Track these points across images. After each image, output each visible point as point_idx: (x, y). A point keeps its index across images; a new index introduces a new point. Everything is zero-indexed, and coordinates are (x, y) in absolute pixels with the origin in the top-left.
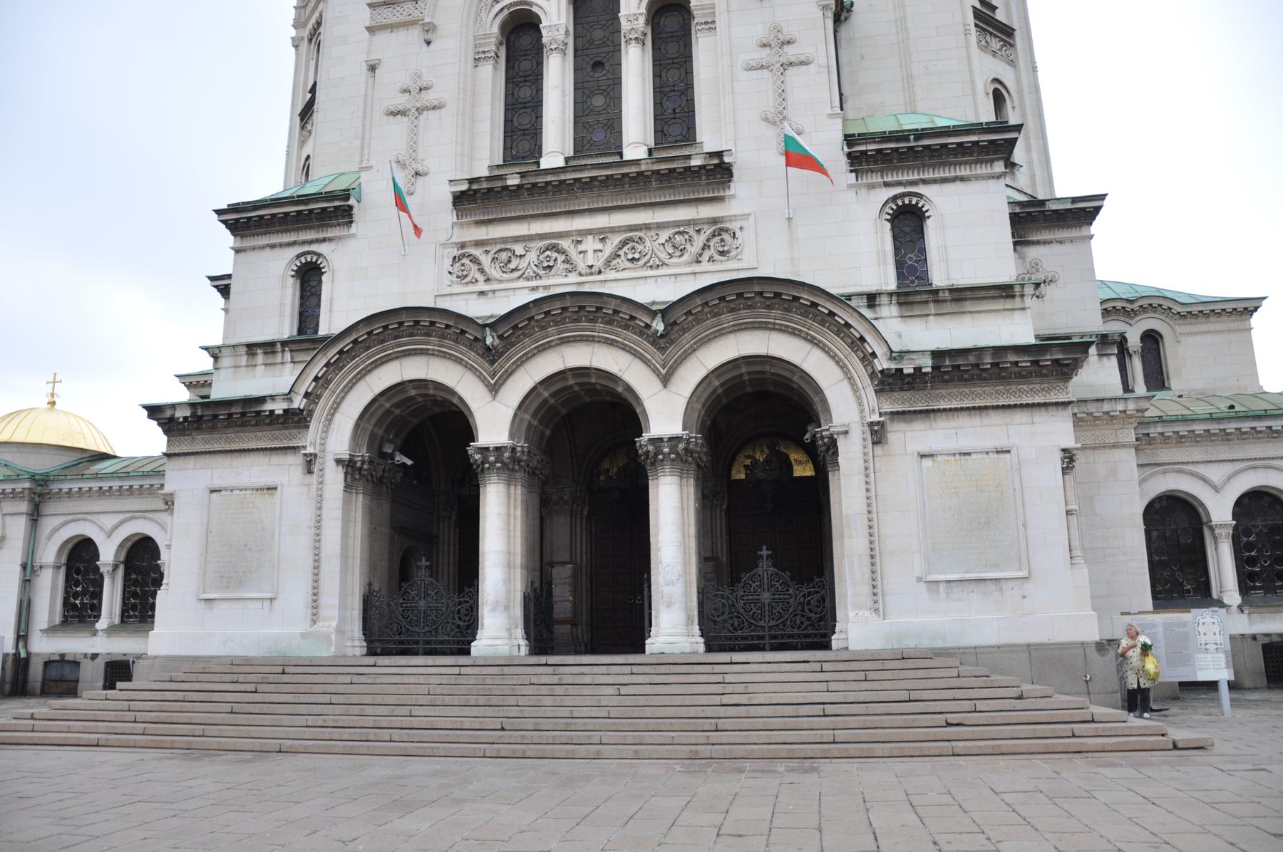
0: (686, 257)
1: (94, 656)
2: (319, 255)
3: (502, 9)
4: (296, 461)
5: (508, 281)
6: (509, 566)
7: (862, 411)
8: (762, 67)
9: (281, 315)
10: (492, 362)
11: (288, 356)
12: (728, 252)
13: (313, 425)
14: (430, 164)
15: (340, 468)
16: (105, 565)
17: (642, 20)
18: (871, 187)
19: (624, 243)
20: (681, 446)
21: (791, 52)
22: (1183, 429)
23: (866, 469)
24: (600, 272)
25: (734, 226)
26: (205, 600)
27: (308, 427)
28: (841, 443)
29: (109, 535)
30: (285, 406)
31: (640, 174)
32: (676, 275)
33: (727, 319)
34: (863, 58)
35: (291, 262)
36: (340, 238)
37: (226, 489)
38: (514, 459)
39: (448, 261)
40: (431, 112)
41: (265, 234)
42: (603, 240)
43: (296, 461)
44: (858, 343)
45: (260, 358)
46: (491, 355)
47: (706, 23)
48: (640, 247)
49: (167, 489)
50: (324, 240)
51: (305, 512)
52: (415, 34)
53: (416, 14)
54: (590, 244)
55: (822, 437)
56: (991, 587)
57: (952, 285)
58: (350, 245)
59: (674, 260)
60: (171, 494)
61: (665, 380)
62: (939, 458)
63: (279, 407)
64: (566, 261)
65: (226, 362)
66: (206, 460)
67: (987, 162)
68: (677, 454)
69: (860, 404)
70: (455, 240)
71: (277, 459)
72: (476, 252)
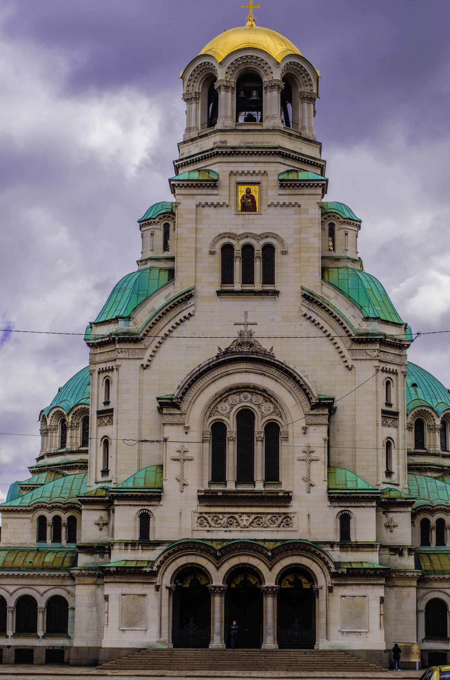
0: (275, 525)
1: (9, 647)
2: (149, 511)
3: (212, 421)
4: (153, 586)
5: (217, 527)
6: (221, 622)
7: (326, 582)
8: (303, 460)
9: (135, 532)
10: (218, 560)
11: (140, 547)
12: (289, 524)
13: (159, 575)
14: (189, 481)
15: (167, 590)
16: (10, 608)
17: (263, 434)
18: (335, 507)
19: (256, 518)
20: (275, 589)
21: (313, 455)
22: (441, 577)
23: (327, 599)
24: (248, 527)
25: (291, 516)
26: (122, 630)
27: (157, 576)
28: (320, 591)
29: (11, 594)
30: (150, 569)
31: (262, 496)
32: (272, 531)
33: (290, 552)
34: (338, 430)
35: (138, 512)
36: (156, 505)
37: (128, 595)
38: (224, 590)
39: (196, 518)
40: (188, 461)
41: (127, 500)
42: (249, 516)
43: (153, 586)
44: (326, 563)
45: (129, 547)
46: (218, 558)
47: (285, 438)
48: (261, 520)
49: (106, 593)
50: (150, 505)
51: (156, 603)
52: (181, 428)
53: (181, 420)
54: (245, 517)
55: (315, 588)
56: (358, 634)
57: (356, 542)
58: (160, 508)
59: (272, 526)
60: (108, 595)
61: (270, 569)
62: (347, 597)
63: (148, 570)
64: (236, 522)
65: (116, 547)
66: (120, 584)
67: (371, 501)
68: (273, 591)
69: (326, 580)
70: (199, 511)
71: (145, 586)
72: (206, 516)
